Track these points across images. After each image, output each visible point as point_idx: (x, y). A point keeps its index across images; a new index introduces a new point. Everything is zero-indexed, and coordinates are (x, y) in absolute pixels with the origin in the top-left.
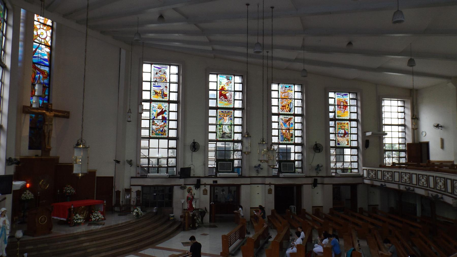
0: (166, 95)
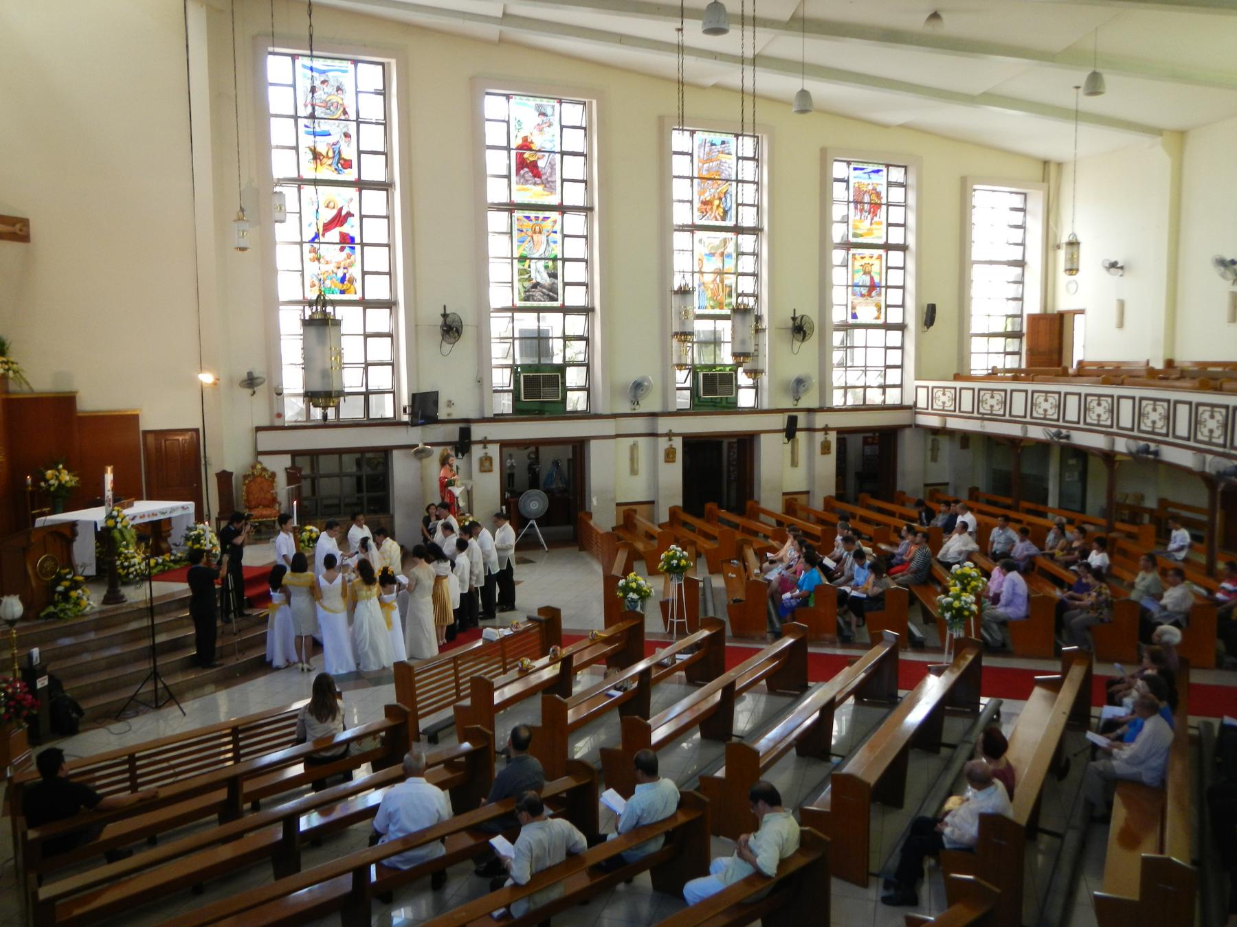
0: (347, 164)
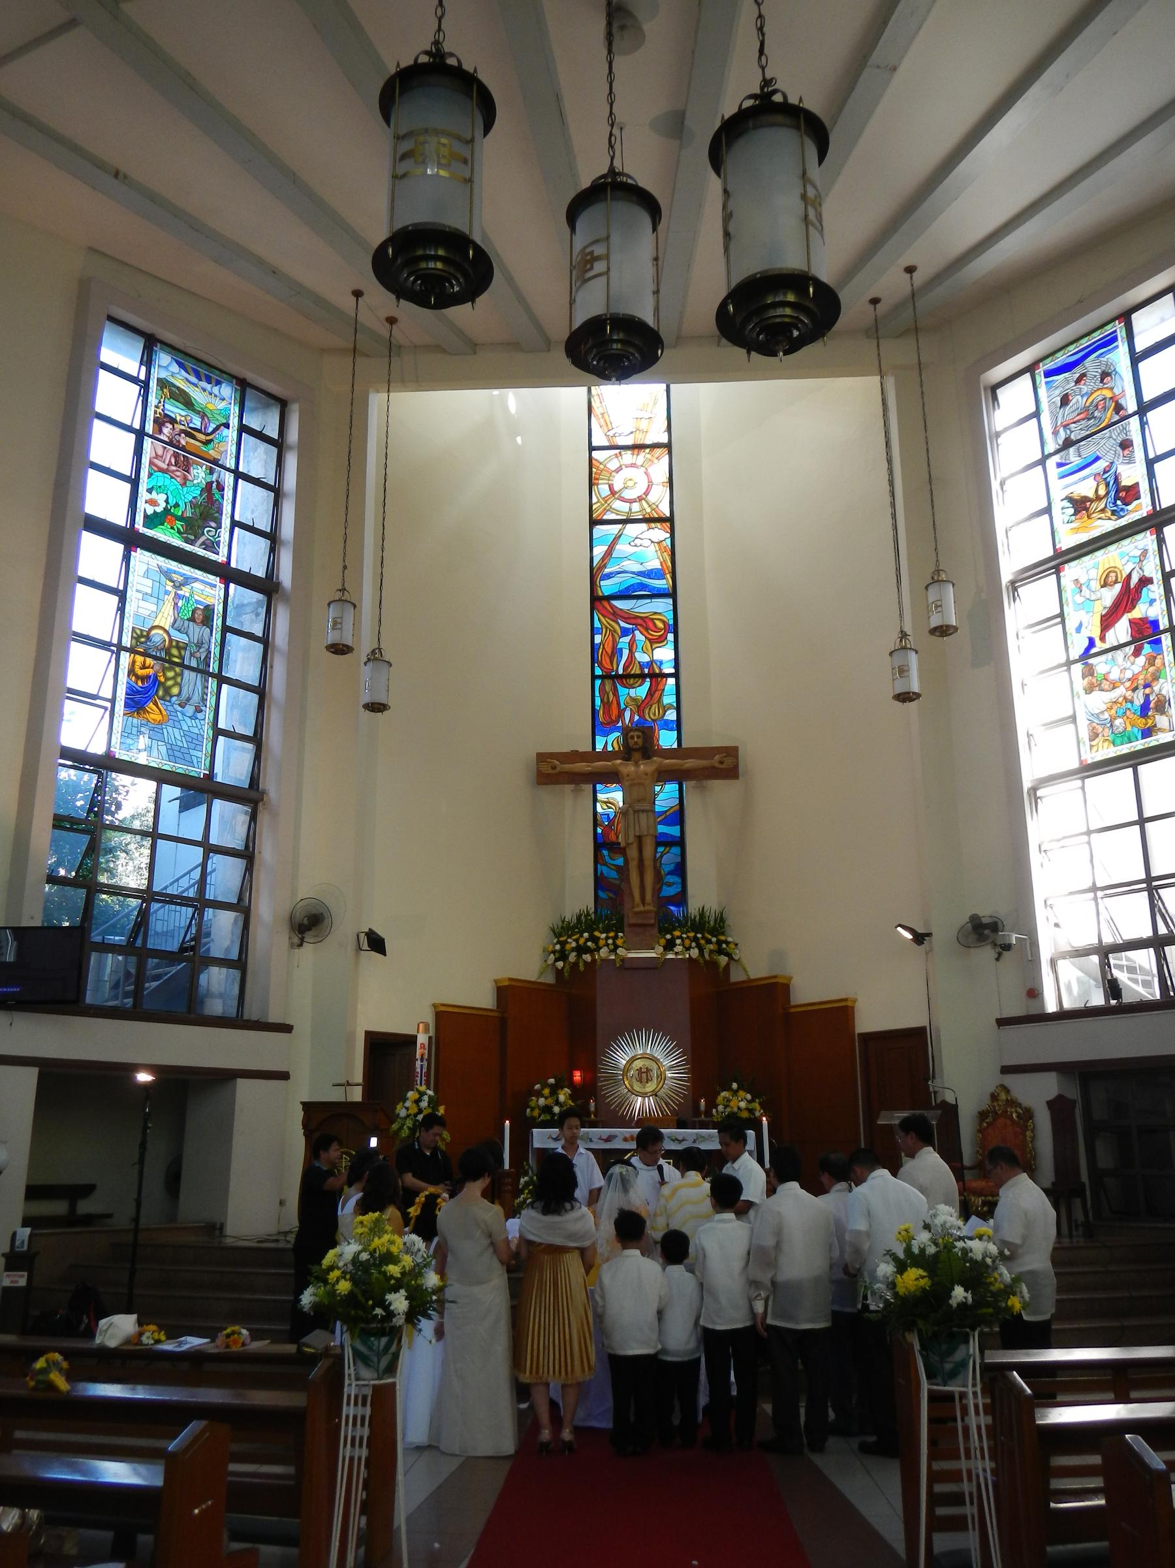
0: (1130, 494)
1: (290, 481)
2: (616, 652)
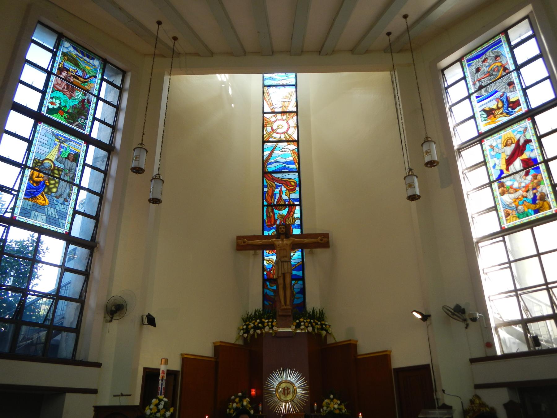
1: (124, 104)
2: (273, 195)
